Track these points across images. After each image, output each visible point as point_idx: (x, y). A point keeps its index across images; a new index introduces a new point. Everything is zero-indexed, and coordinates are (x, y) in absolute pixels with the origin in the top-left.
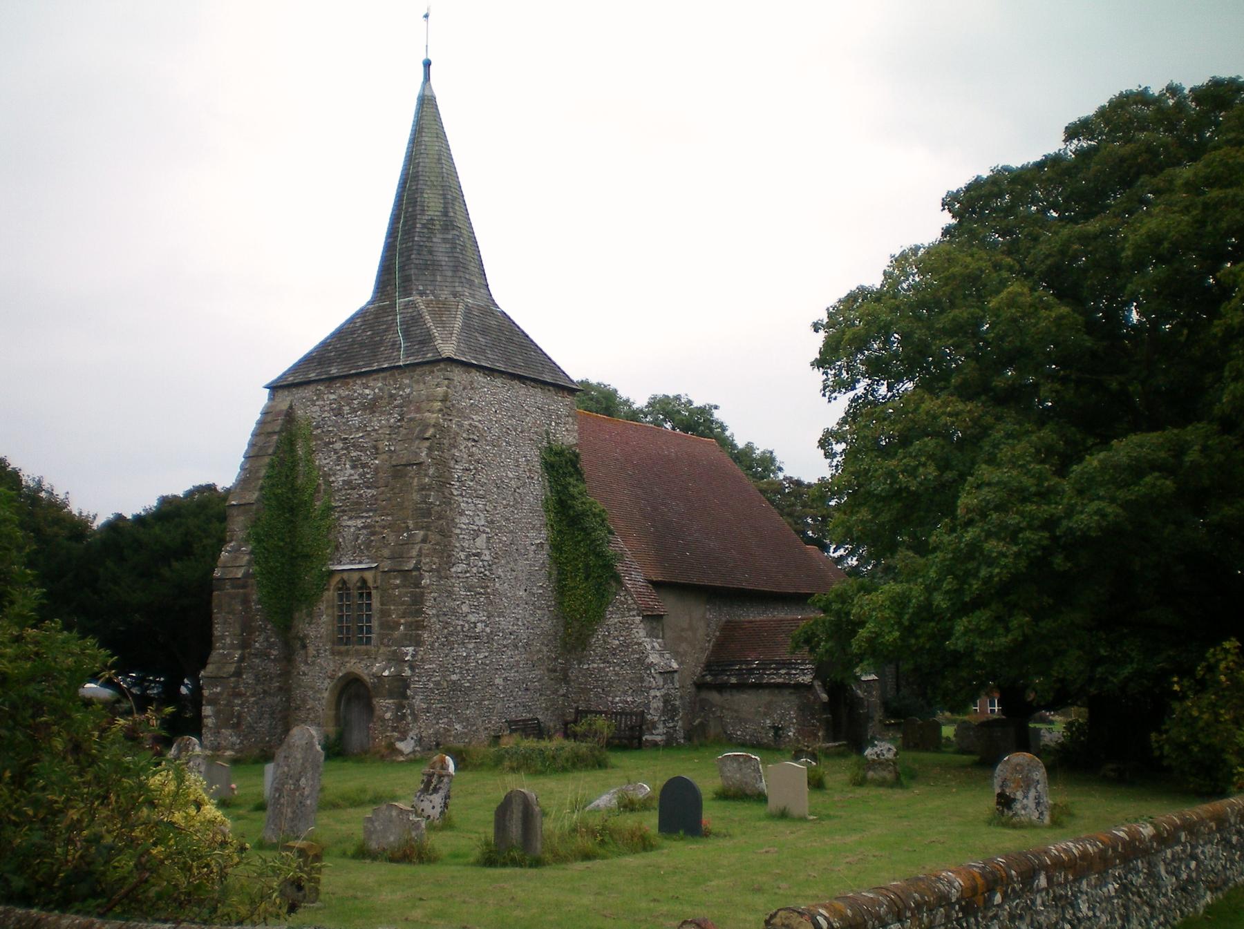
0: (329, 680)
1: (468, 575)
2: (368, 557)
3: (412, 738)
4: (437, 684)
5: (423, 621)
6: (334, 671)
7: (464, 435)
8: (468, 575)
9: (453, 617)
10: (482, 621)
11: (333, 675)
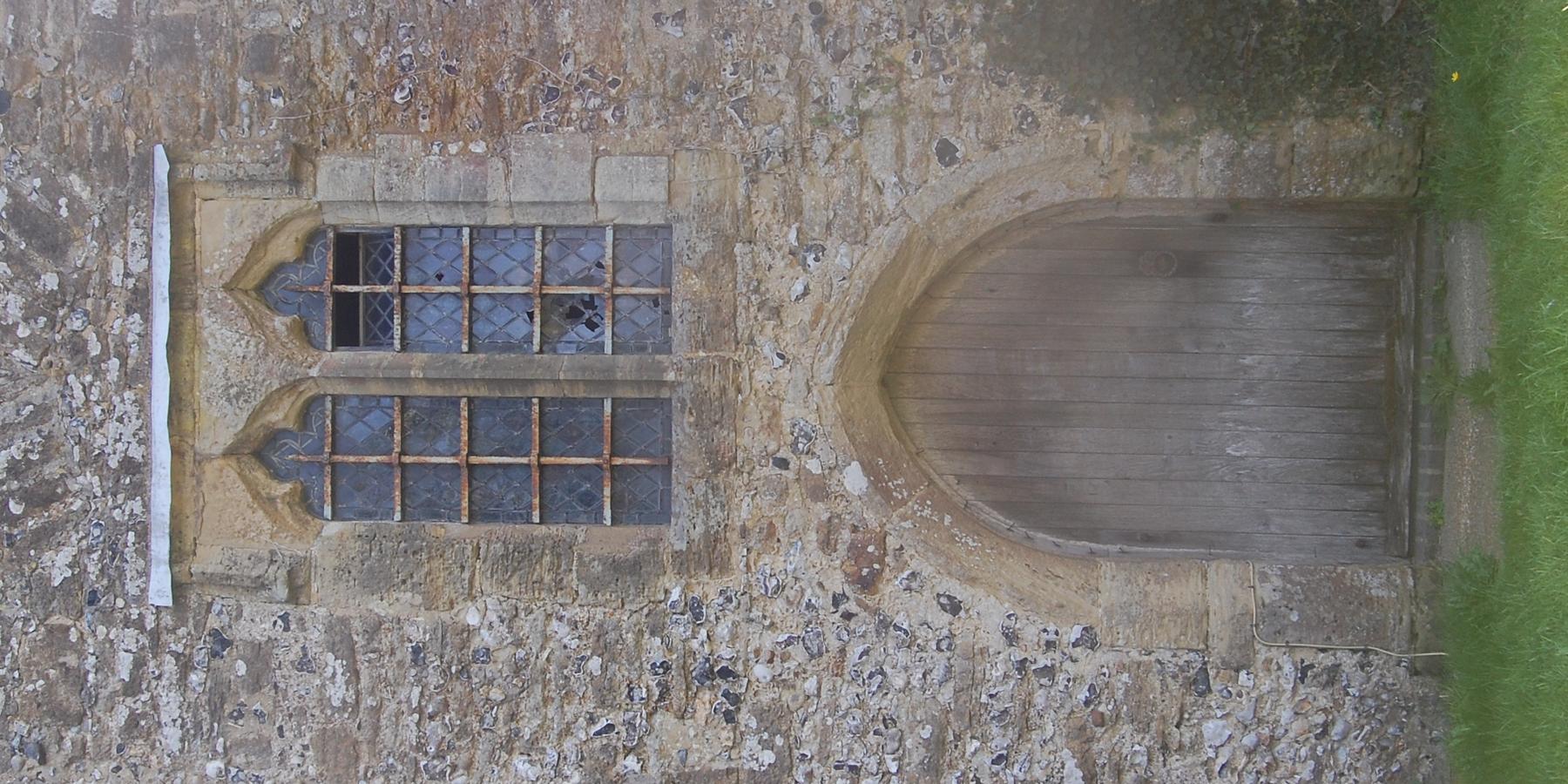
0: (890, 589)
2: (108, 234)
6: (827, 545)
11: (857, 551)
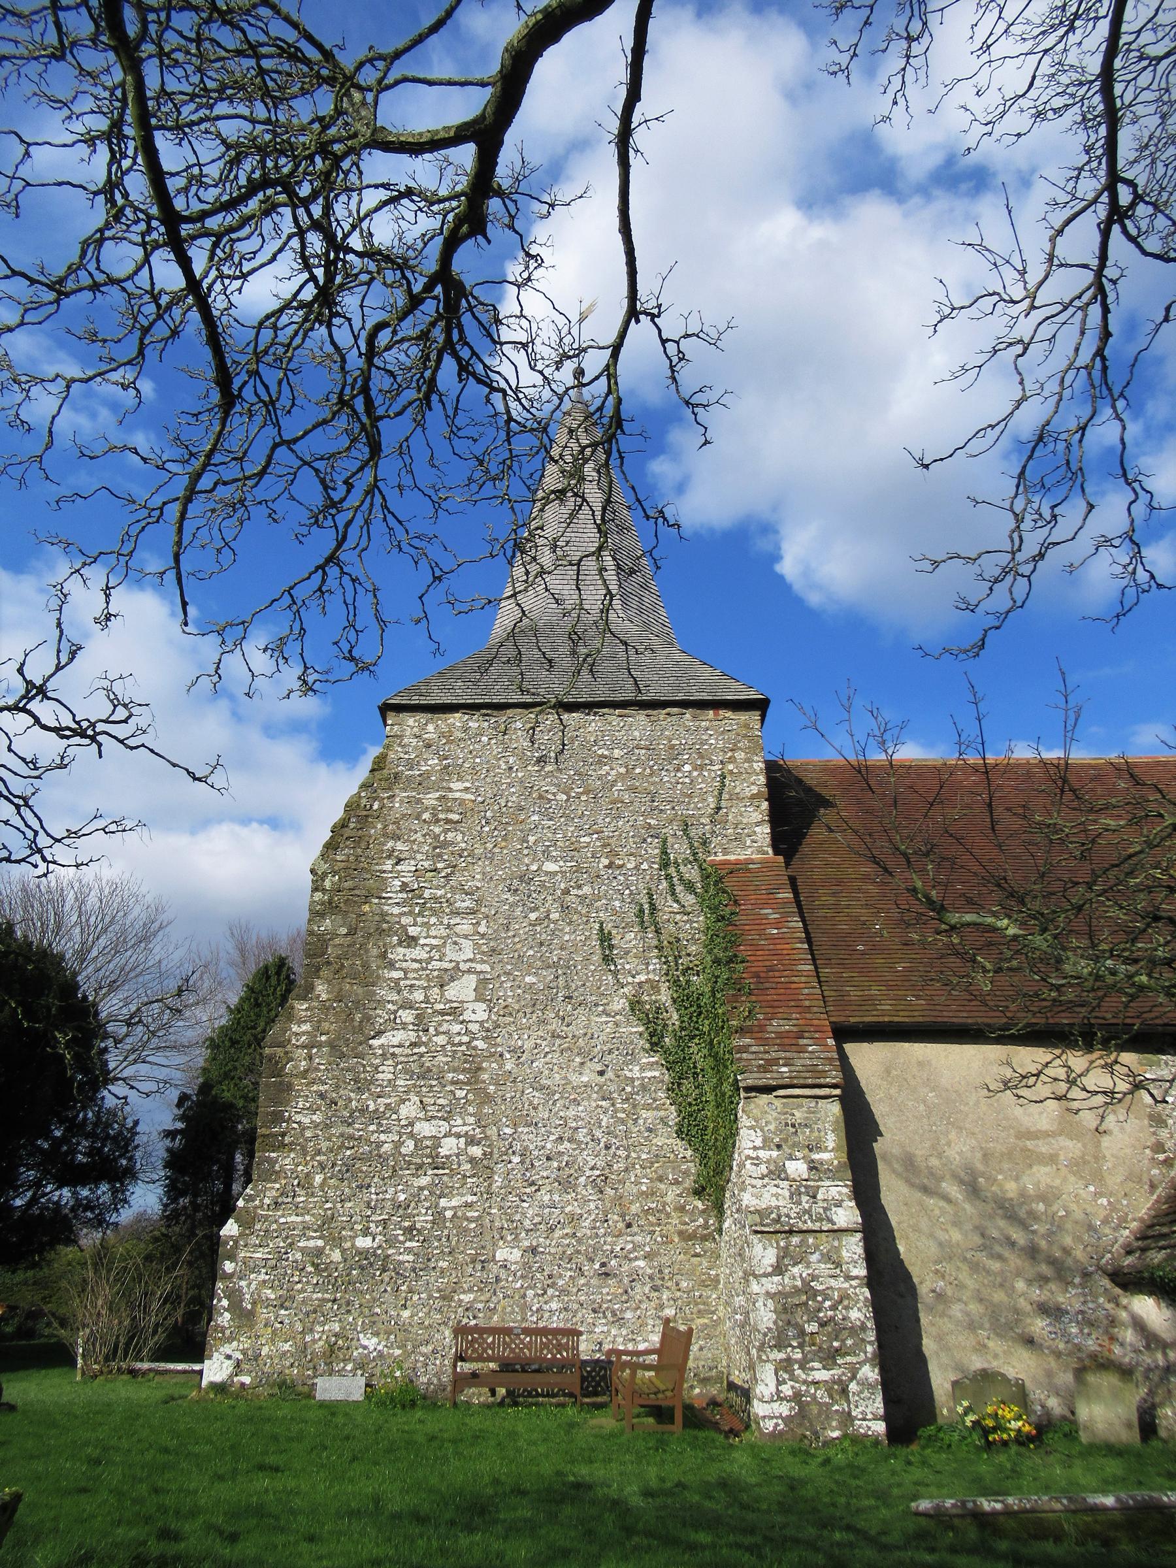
1: (423, 1049)
3: (229, 1357)
4: (319, 1252)
5: (283, 1135)
7: (426, 816)
8: (423, 1049)
9: (372, 1128)
10: (458, 1136)
